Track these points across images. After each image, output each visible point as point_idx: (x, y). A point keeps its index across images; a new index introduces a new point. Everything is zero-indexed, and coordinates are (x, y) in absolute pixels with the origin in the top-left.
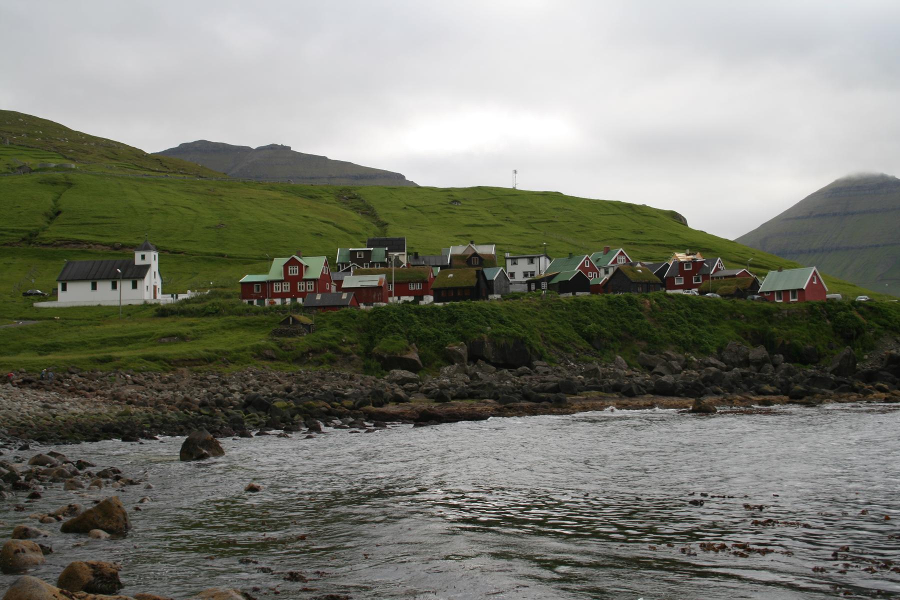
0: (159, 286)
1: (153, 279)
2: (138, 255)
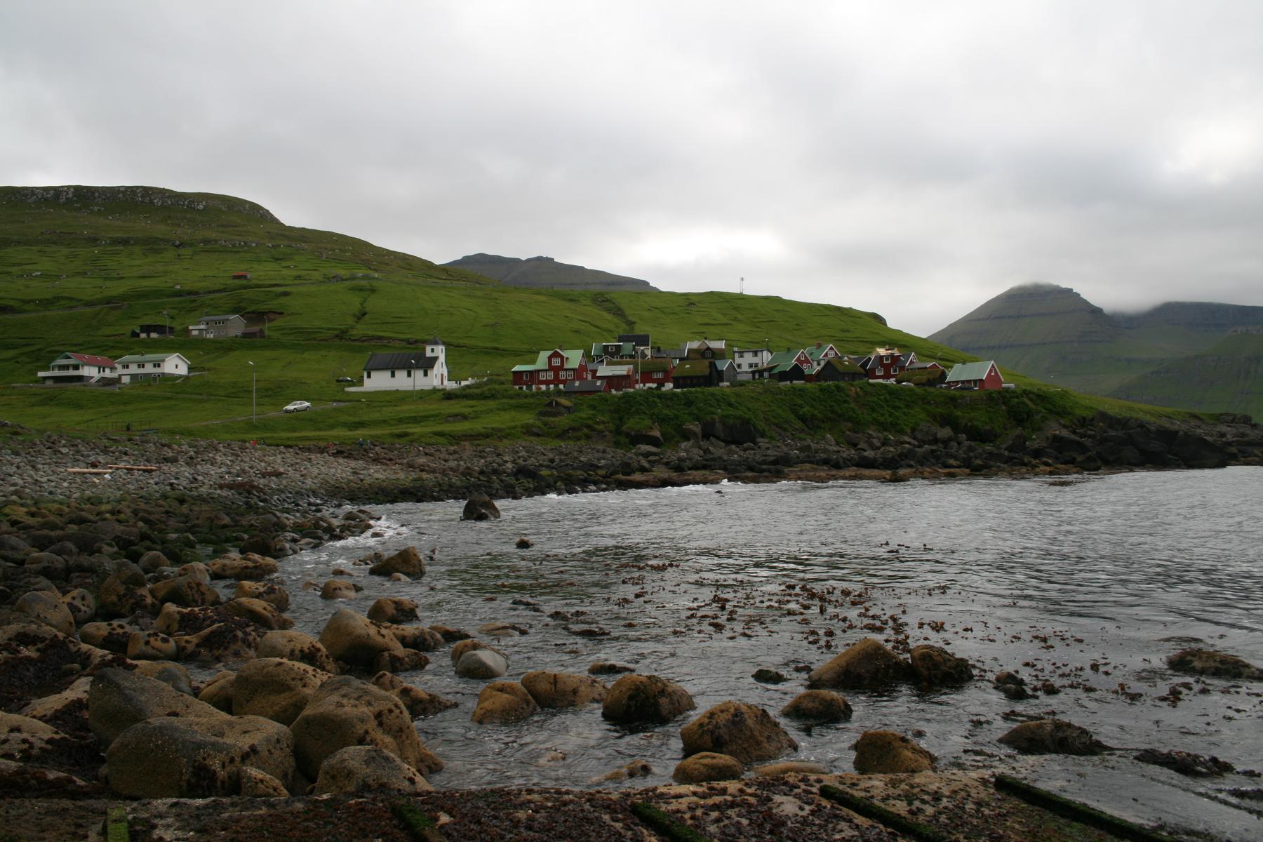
0: (446, 374)
1: (440, 369)
2: (428, 349)
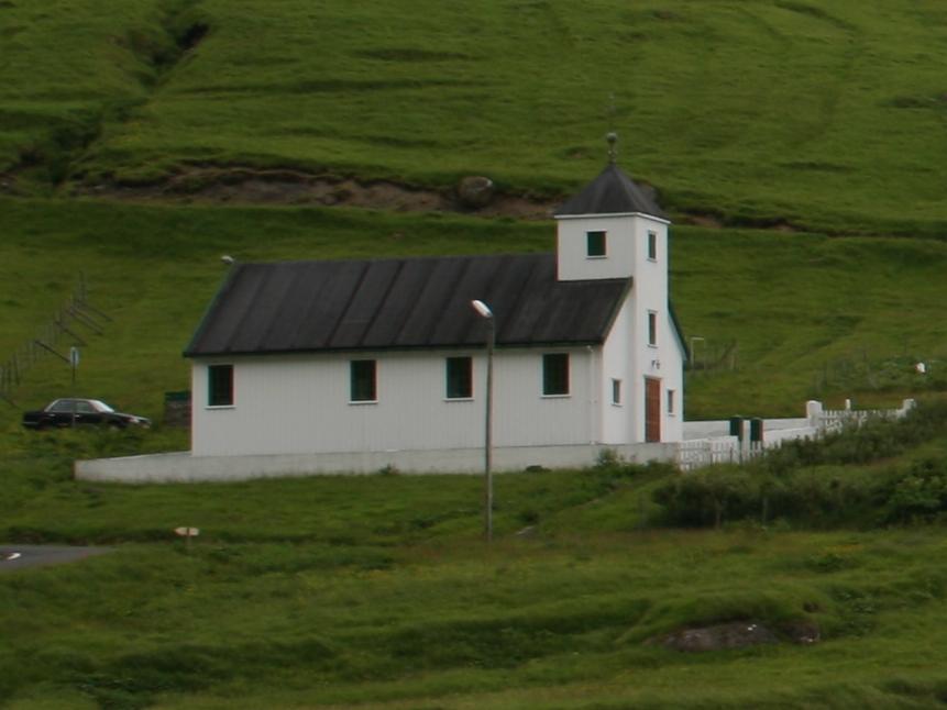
0: (672, 379)
1: (641, 350)
2: (571, 235)
